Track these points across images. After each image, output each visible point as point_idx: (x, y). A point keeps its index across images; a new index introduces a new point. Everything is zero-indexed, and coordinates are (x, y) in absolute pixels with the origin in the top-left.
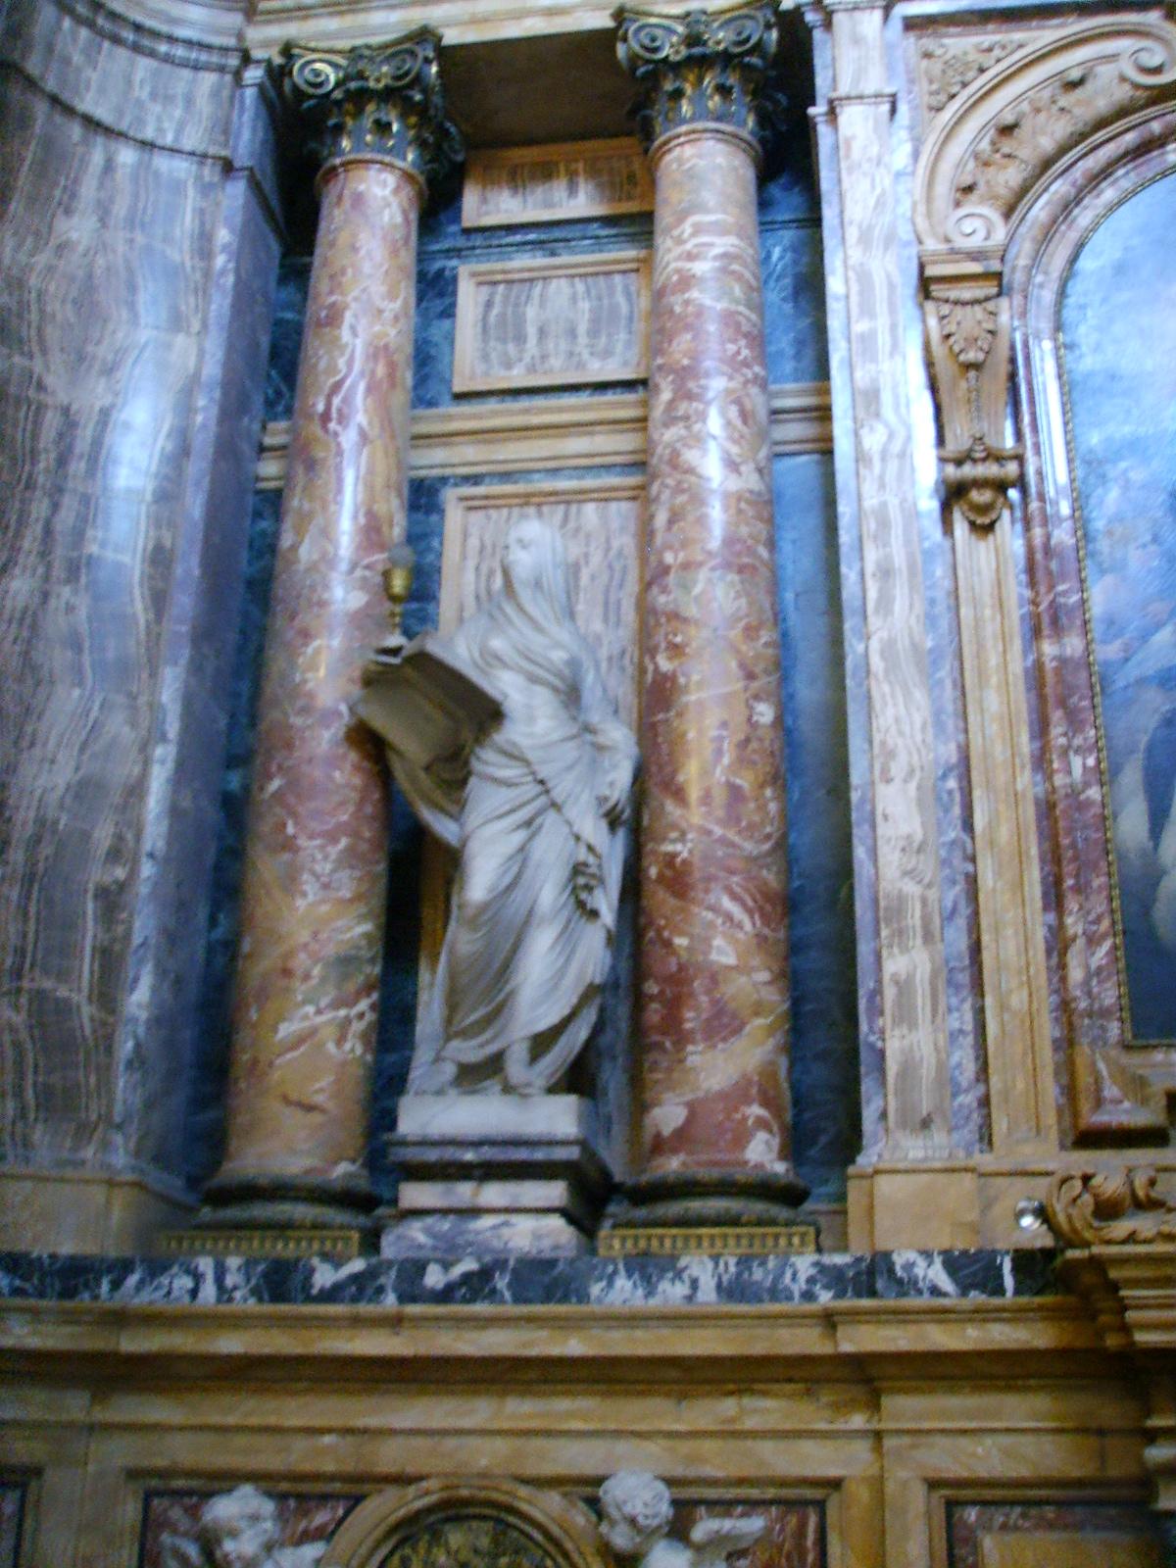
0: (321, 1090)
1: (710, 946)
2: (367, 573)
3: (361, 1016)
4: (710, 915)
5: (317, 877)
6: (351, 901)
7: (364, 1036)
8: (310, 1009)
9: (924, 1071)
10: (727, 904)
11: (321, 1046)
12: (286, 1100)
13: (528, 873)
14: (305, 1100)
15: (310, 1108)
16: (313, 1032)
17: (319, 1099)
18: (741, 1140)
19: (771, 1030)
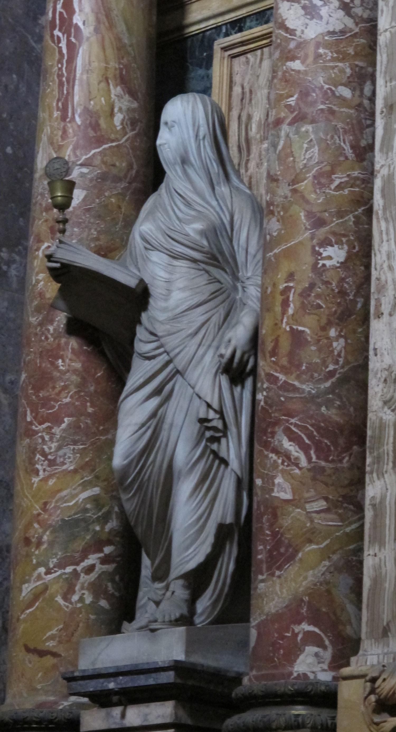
0: (52, 638)
1: (273, 484)
2: (85, 170)
3: (90, 569)
4: (273, 456)
5: (44, 454)
6: (75, 471)
7: (96, 589)
8: (42, 570)
9: (387, 585)
10: (287, 445)
11: (52, 598)
12: (28, 650)
13: (164, 435)
14: (41, 647)
15: (42, 653)
16: (46, 588)
17: (51, 644)
18: (293, 653)
19: (325, 554)
